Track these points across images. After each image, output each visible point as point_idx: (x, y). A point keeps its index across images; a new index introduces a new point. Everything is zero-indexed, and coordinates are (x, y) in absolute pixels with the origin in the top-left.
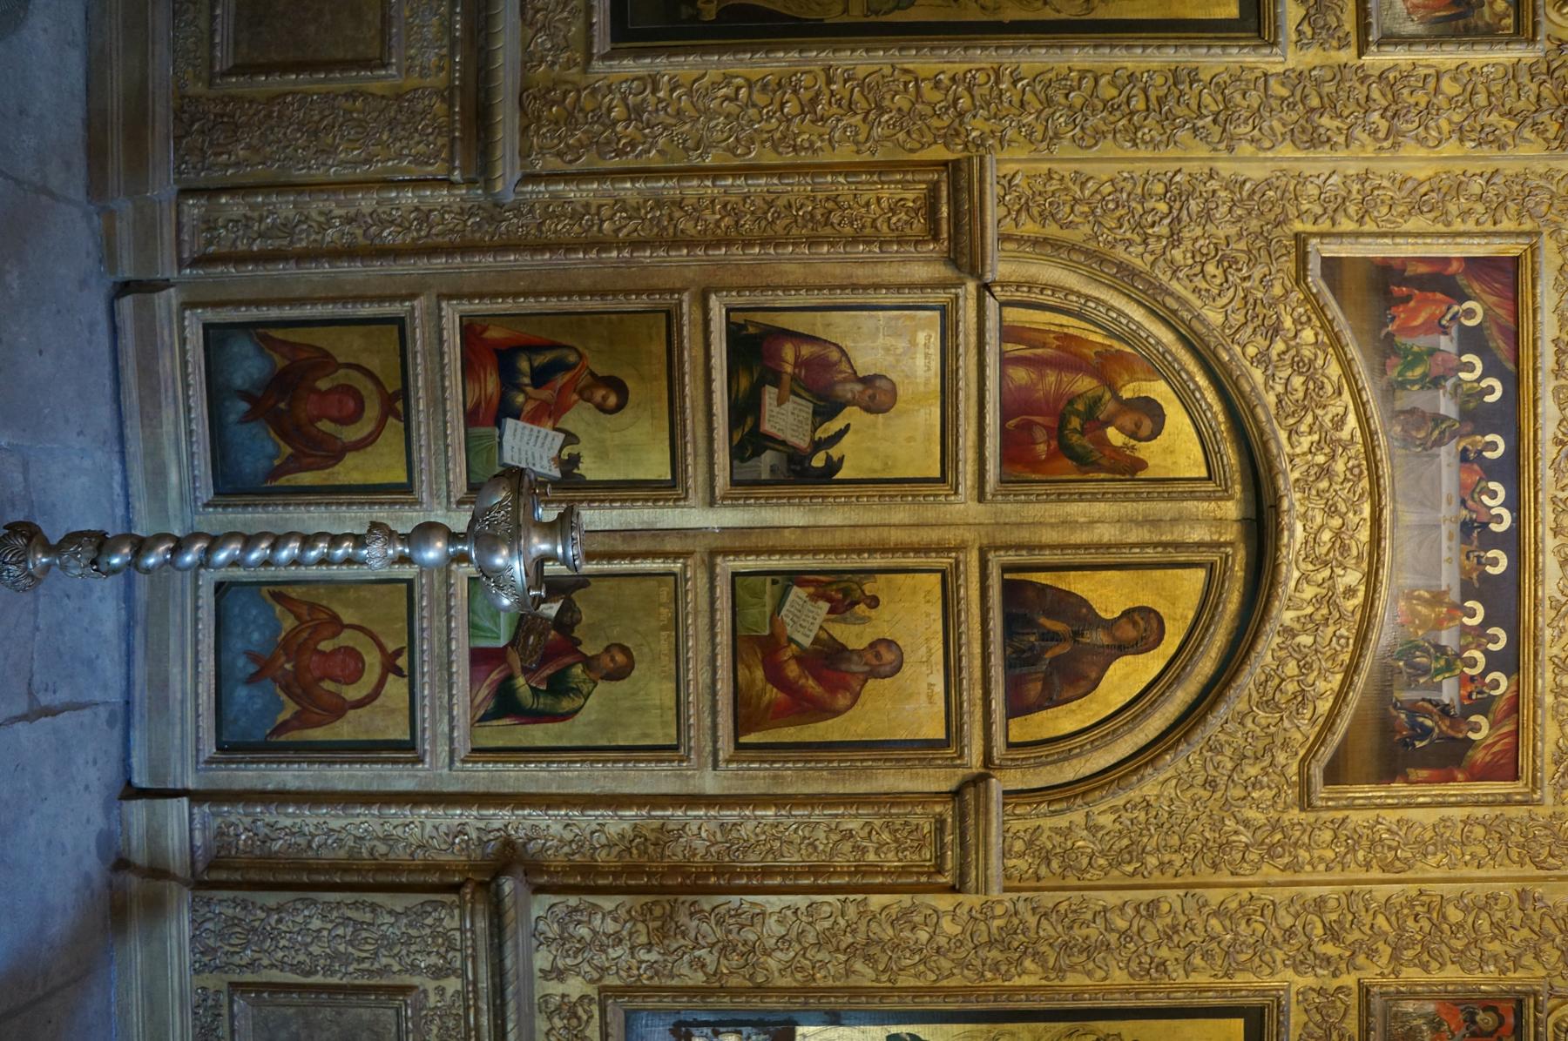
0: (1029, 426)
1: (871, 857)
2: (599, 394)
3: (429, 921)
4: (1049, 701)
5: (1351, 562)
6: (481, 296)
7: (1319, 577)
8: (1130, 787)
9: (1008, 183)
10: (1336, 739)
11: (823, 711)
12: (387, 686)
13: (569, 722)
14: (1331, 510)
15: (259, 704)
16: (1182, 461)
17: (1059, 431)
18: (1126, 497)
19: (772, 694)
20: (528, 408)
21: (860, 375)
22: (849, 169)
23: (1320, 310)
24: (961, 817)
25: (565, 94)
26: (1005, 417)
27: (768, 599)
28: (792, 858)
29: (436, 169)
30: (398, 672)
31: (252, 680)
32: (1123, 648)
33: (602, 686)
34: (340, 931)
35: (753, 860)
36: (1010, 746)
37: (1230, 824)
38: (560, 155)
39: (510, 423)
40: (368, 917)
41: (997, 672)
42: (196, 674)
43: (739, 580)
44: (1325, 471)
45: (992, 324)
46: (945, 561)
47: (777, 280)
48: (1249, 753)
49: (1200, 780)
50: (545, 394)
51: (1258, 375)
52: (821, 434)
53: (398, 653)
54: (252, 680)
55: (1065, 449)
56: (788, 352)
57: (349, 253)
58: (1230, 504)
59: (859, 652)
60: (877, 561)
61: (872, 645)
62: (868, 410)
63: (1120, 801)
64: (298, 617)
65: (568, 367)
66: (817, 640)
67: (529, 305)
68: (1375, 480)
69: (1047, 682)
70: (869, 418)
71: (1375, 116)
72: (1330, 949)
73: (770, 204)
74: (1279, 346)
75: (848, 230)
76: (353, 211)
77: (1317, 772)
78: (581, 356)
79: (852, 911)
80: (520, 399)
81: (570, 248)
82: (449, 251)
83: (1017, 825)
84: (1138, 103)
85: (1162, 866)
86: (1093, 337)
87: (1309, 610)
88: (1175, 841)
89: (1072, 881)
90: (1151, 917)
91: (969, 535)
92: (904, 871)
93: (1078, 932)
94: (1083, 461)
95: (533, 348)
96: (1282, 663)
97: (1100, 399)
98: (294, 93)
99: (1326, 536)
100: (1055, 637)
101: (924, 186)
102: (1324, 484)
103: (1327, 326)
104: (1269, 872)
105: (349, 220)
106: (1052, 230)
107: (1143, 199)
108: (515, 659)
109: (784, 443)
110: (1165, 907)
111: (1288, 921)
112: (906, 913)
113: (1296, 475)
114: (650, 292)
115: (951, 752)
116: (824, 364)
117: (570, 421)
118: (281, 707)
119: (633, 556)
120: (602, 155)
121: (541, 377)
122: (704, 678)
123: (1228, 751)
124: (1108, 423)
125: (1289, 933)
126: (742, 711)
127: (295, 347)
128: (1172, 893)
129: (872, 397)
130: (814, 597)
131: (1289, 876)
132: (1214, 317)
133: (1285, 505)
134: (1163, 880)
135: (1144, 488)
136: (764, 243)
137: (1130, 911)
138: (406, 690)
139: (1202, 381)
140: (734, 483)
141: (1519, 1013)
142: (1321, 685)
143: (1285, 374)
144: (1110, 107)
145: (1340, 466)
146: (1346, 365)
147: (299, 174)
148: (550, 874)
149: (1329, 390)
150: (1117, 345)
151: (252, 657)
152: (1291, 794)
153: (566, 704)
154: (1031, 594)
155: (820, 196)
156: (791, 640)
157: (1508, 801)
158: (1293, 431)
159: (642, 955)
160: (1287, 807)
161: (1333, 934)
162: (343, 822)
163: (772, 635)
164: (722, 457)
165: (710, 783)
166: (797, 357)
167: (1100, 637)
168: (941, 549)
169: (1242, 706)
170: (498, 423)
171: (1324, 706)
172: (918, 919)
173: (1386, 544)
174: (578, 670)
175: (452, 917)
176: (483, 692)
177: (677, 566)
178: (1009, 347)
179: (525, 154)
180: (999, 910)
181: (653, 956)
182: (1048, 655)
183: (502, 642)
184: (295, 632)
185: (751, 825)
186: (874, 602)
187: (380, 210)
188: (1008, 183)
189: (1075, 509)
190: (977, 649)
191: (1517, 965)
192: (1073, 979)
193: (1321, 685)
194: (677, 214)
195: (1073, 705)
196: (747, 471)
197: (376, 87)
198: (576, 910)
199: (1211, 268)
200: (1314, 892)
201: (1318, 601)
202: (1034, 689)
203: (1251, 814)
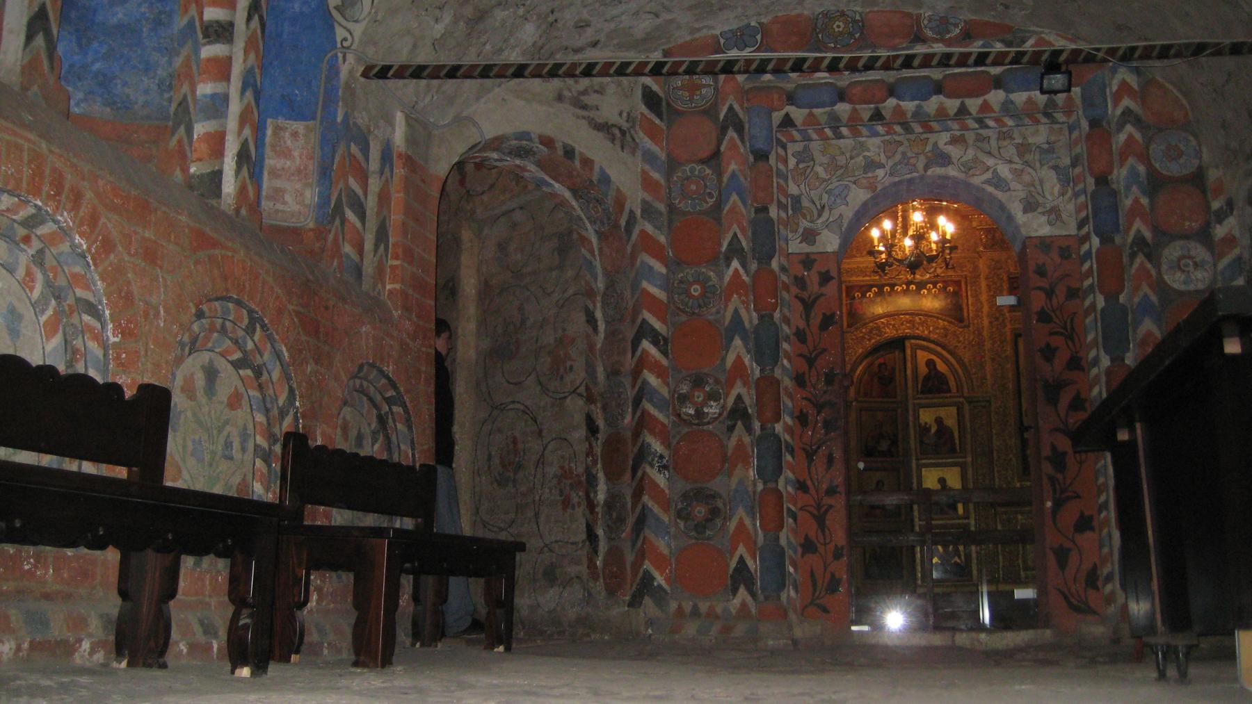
11: (952, 433)
14: (902, 324)
44: (894, 326)
51: (873, 341)
72: (1001, 319)
77: (963, 325)
111: (994, 330)
125: (997, 329)
132: (860, 351)
141: (1013, 278)
152: (966, 330)
157: (966, 283)
158: (885, 333)
161: (997, 319)
171: (946, 323)
186: (926, 423)
191: (1002, 279)
192: (1010, 376)
201: (923, 326)
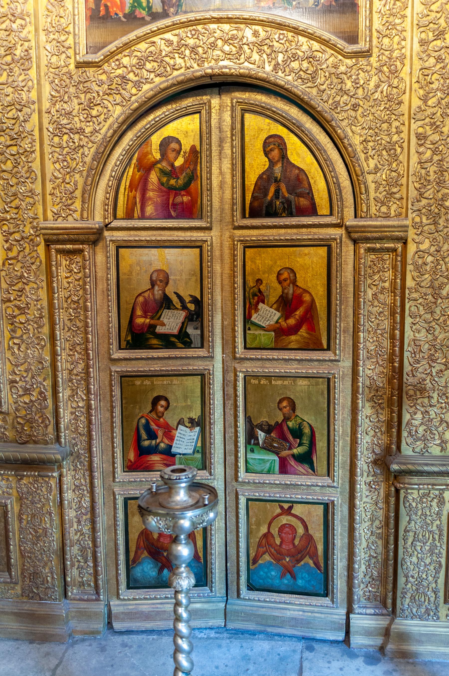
0: (174, 205)
1: (387, 285)
2: (160, 409)
3: (414, 504)
4: (310, 195)
5: (240, 34)
6: (114, 463)
7: (248, 51)
8: (355, 151)
9: (57, 215)
10: (334, 39)
11: (311, 307)
12: (297, 514)
13: (315, 429)
14: (213, 46)
15: (305, 575)
16: (191, 127)
17: (175, 190)
18: (210, 156)
19: (303, 331)
20: (166, 441)
21: (150, 287)
22: (51, 291)
23: (112, 54)
24: (367, 240)
25: (19, 423)
26: (169, 217)
27: (257, 333)
28: (386, 324)
29: (53, 483)
30: (291, 508)
31: (294, 577)
32: (284, 156)
33: (298, 413)
34: (419, 548)
35: (386, 343)
36: (331, 214)
37: (377, 95)
38: (46, 426)
39: (174, 450)
40: (411, 534)
41: (294, 221)
42: (290, 603)
43: (248, 346)
44: (193, 49)
45: (124, 223)
46: (240, 247)
47: (105, 327)
48: (339, 87)
49: (352, 113)
50: (160, 433)
51: (146, 87)
52: (179, 306)
53: (282, 508)
54: (294, 577)
55: (186, 187)
56: (140, 321)
57: (93, 522)
58: (213, 102)
59: (283, 289)
60: (239, 280)
61: (280, 282)
62: (167, 283)
63: (362, 156)
64: (264, 553)
65: (148, 422)
66: (277, 310)
67: (118, 441)
68: (198, 22)
69: (300, 195)
70: (171, 282)
71: (15, 26)
73: (69, 329)
74: (131, 76)
75: (81, 293)
76: (75, 520)
78: (142, 417)
79: (415, 295)
80: (162, 445)
81: (90, 422)
82: (92, 478)
83: (373, 210)
84: (14, 150)
85: (399, 132)
86: (130, 173)
87: (265, 56)
88: (385, 126)
89: (404, 181)
90: (425, 138)
91: (227, 234)
92: (394, 268)
93: (432, 177)
94: (192, 178)
95: (138, 439)
96: (292, 71)
97: (160, 169)
98: (20, 546)
99: (227, 48)
100: (277, 192)
101: (59, 256)
102: (200, 50)
103: (120, 50)
104: (405, 73)
105: (79, 522)
106: (78, 193)
107: (62, 147)
108: (285, 453)
109: (183, 323)
110: (421, 130)
111: (432, 61)
112: (417, 268)
113: (195, 66)
114: (111, 385)
115: (334, 244)
116: (145, 304)
117: (173, 422)
118: (307, 564)
119: (236, 396)
120: (46, 407)
121: (152, 435)
122: (295, 365)
123: (338, 98)
124: (172, 165)
125: (439, 59)
126: (311, 347)
127: (138, 548)
128: (413, 126)
129: (161, 281)
130: (257, 310)
131: (407, 62)
132: (119, 110)
133: (209, 71)
134: (406, 132)
135: (205, 147)
136: (86, 333)
137: (421, 149)
138: (299, 505)
139: (151, 117)
140: (202, 347)
142: (305, 48)
143: (145, 73)
144: (16, 164)
145: (191, 42)
146: (140, 40)
147: (55, 545)
148: (391, 444)
149: (152, 49)
150: (134, 161)
151: (283, 576)
152: (362, 61)
153: (307, 431)
154: (256, 204)
155: (65, 305)
156: (277, 322)
159: (434, 401)
160: (369, 64)
162: (364, 540)
163: (274, 331)
164: (190, 352)
165: (347, 364)
166: (142, 317)
167: (278, 169)
168: (233, 248)
169: (314, 91)
170: (174, 455)
171: (316, 46)
172: (420, 261)
173: (230, 14)
174: (290, 424)
175: (412, 493)
176: (300, 469)
177: (241, 375)
178: (136, 215)
179: (46, 443)
180: (417, 219)
181: (435, 395)
182: (287, 195)
183: (276, 458)
184: (271, 555)
185: (368, 344)
186: (259, 281)
187: (75, 507)
188: (57, 215)
189: (215, 182)
190: (282, 231)
193: (305, 48)
194: (75, 372)
195: (312, 181)
196: (197, 341)
197: (16, 509)
198: (410, 433)
199: (94, 113)
200: (416, 46)
201: (260, 52)
202: (303, 202)
203: (372, 84)
